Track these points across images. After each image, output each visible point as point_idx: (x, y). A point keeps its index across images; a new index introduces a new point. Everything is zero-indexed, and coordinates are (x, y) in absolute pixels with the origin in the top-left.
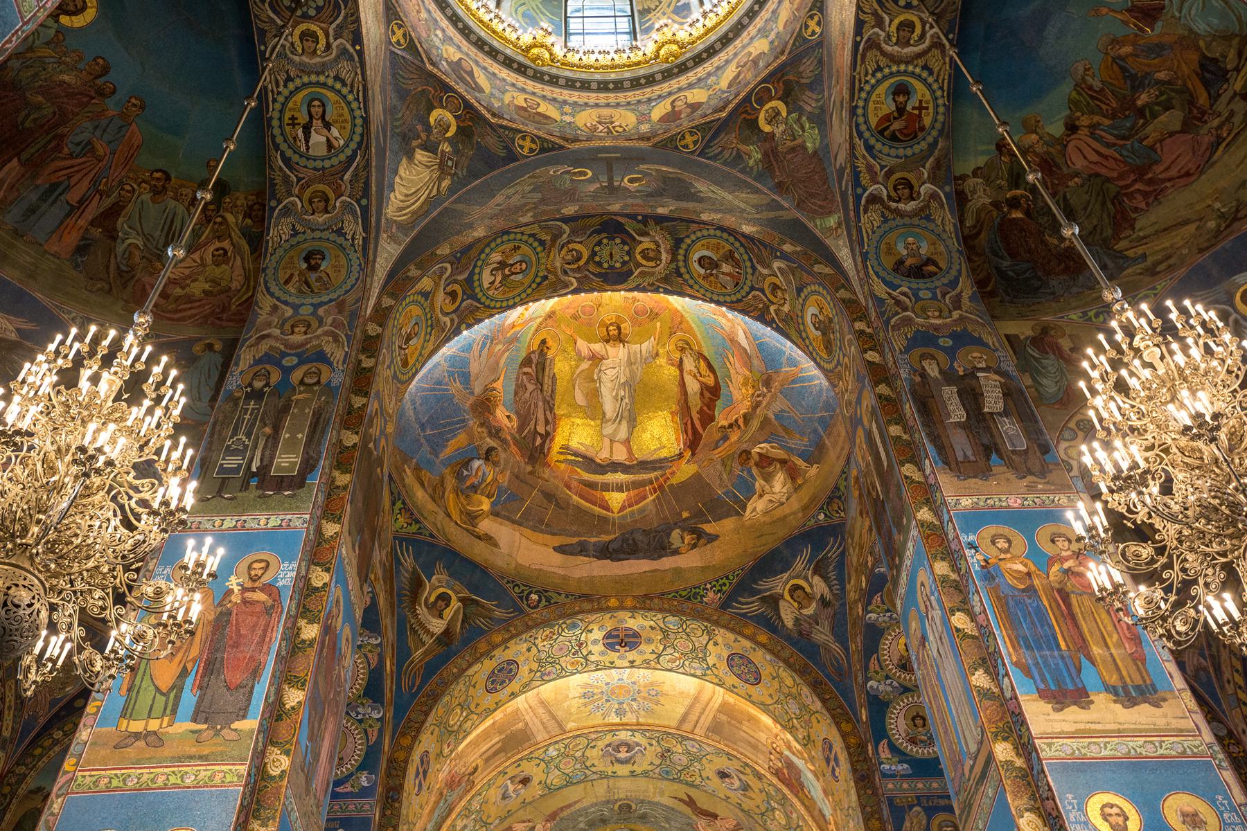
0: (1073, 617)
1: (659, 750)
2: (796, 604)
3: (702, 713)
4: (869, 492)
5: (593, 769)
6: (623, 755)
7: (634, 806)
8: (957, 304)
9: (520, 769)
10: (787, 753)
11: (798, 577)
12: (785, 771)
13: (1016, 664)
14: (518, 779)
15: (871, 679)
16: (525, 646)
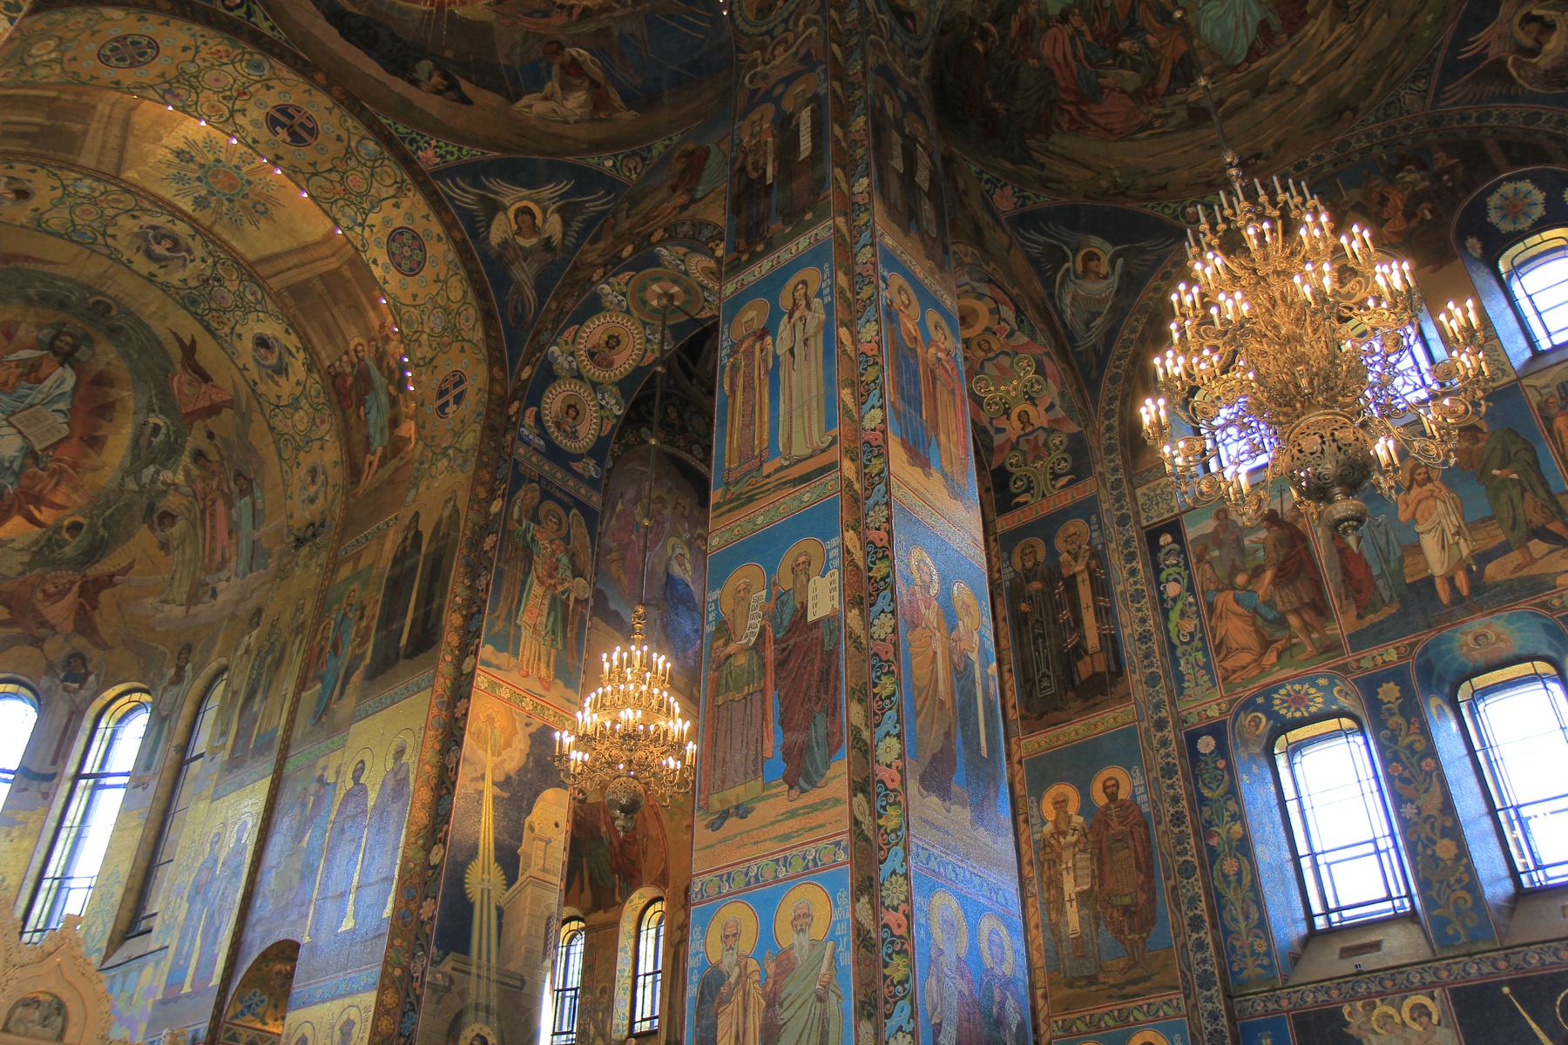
0: (935, 400)
1: (208, 272)
2: (515, 227)
3: (297, 266)
4: (743, 169)
5: (110, 241)
6: (159, 250)
7: (114, 312)
8: (915, 72)
9: (31, 176)
10: (371, 364)
11: (537, 202)
12: (350, 380)
13: (892, 404)
14: (17, 186)
15: (557, 344)
16: (186, 40)
